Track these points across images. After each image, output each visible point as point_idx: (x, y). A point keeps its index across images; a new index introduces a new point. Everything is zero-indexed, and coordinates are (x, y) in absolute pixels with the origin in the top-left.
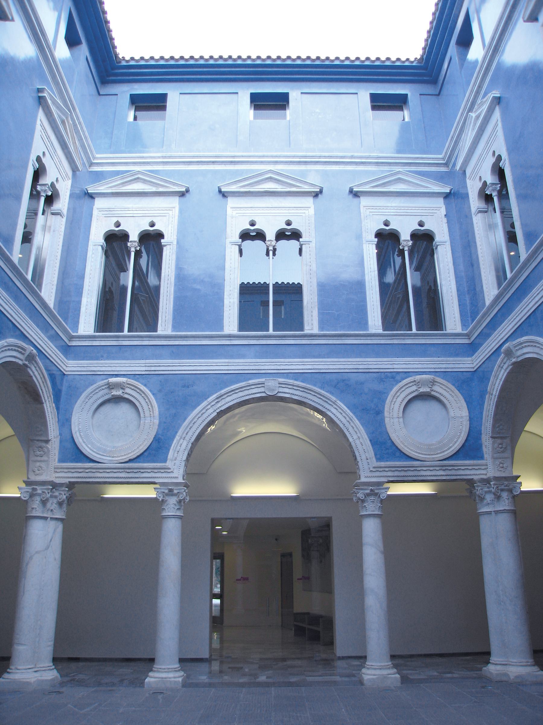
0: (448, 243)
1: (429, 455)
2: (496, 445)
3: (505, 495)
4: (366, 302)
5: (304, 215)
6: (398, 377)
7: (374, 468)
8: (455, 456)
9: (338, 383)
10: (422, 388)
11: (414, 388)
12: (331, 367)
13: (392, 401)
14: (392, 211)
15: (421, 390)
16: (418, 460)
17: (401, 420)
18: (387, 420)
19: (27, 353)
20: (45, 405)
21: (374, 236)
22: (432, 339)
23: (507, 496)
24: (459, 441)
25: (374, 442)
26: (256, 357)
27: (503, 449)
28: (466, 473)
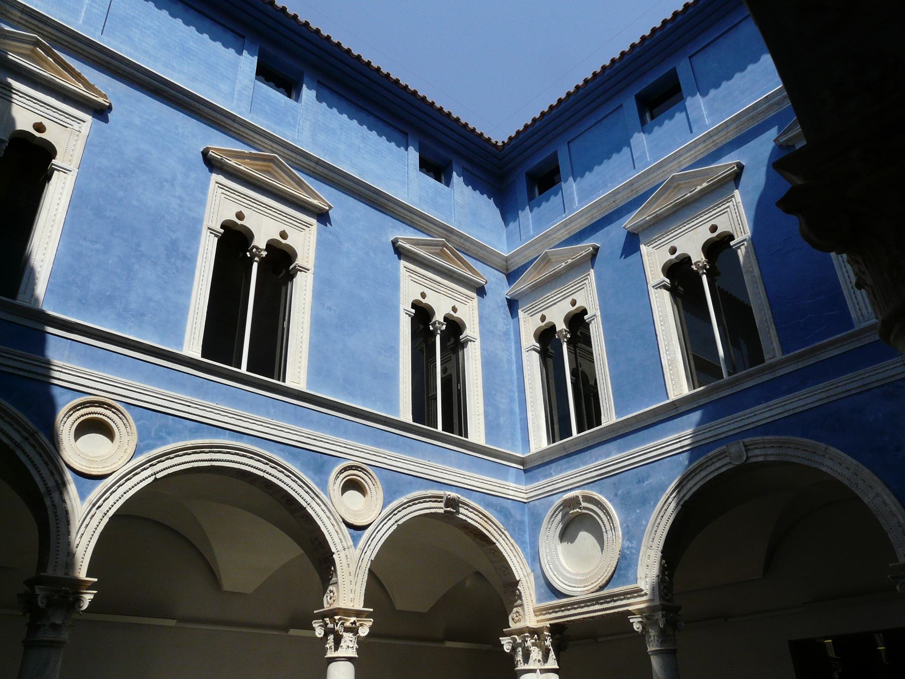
19: (444, 500)
20: (498, 544)
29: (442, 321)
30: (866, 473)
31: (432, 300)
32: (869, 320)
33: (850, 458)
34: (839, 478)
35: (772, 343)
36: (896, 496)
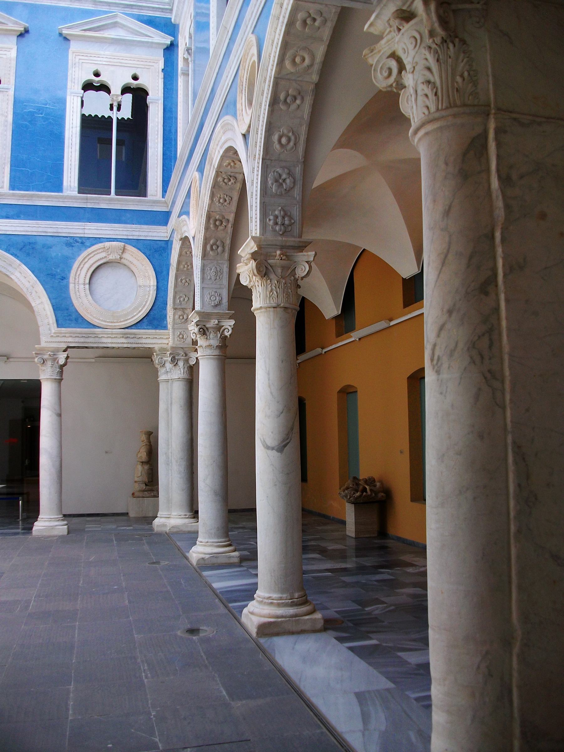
0: (161, 102)
1: (112, 322)
2: (177, 317)
3: (181, 364)
4: (63, 161)
6: (88, 244)
7: (55, 333)
8: (138, 325)
9: (24, 246)
10: (111, 255)
11: (103, 255)
12: (18, 229)
13: (78, 267)
14: (105, 59)
15: (111, 257)
16: (99, 327)
17: (87, 286)
18: (71, 286)
21: (80, 87)
22: (131, 203)
24: (144, 310)
25: (56, 308)
30: (40, 288)
32: (73, 191)
33: (33, 275)
34: (21, 286)
35: (3, 177)
36: (53, 306)
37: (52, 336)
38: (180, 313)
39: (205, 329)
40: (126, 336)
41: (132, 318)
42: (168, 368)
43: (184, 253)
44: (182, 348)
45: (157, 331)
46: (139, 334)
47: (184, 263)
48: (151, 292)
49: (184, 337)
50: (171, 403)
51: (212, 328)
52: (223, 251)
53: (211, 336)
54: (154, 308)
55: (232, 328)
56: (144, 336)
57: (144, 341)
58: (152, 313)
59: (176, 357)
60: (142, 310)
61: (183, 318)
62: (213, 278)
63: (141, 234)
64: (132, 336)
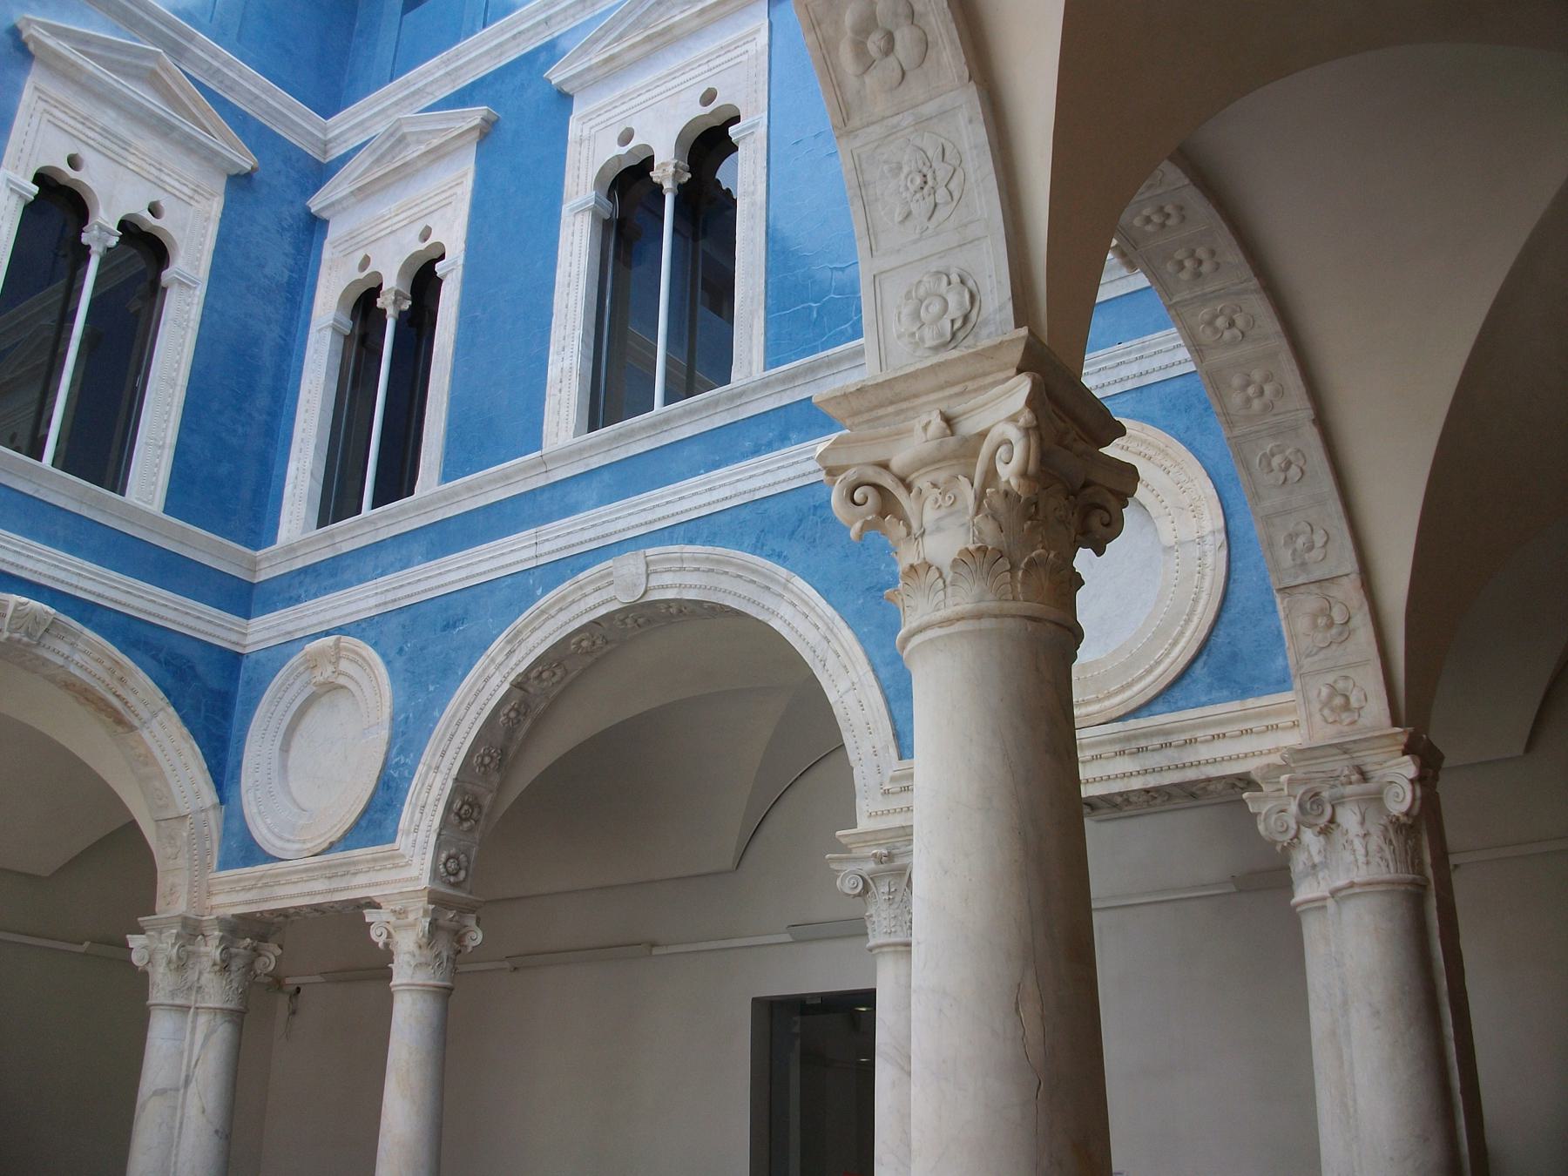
5: (745, 58)
7: (893, 779)
12: (783, 475)
23: (1363, 823)
26: (601, 502)
27: (1334, 631)
28: (1218, 755)
29: (114, 228)
31: (94, 178)
35: (750, 350)
37: (887, 793)
38: (1311, 602)
39: (887, 481)
40: (1134, 745)
41: (1149, 671)
42: (1314, 850)
43: (1206, 336)
44: (1343, 749)
45: (1251, 703)
46: (1182, 730)
47: (1236, 381)
48: (1209, 560)
49: (1354, 703)
50: (1345, 1003)
51: (924, 464)
52: (925, 45)
53: (930, 515)
54: (1226, 617)
55: (1027, 431)
56: (1199, 734)
57: (1204, 752)
58: (1221, 637)
59: (1325, 794)
60: (1182, 633)
61: (1331, 624)
62: (920, 208)
63: (1146, 365)
64: (1157, 742)
